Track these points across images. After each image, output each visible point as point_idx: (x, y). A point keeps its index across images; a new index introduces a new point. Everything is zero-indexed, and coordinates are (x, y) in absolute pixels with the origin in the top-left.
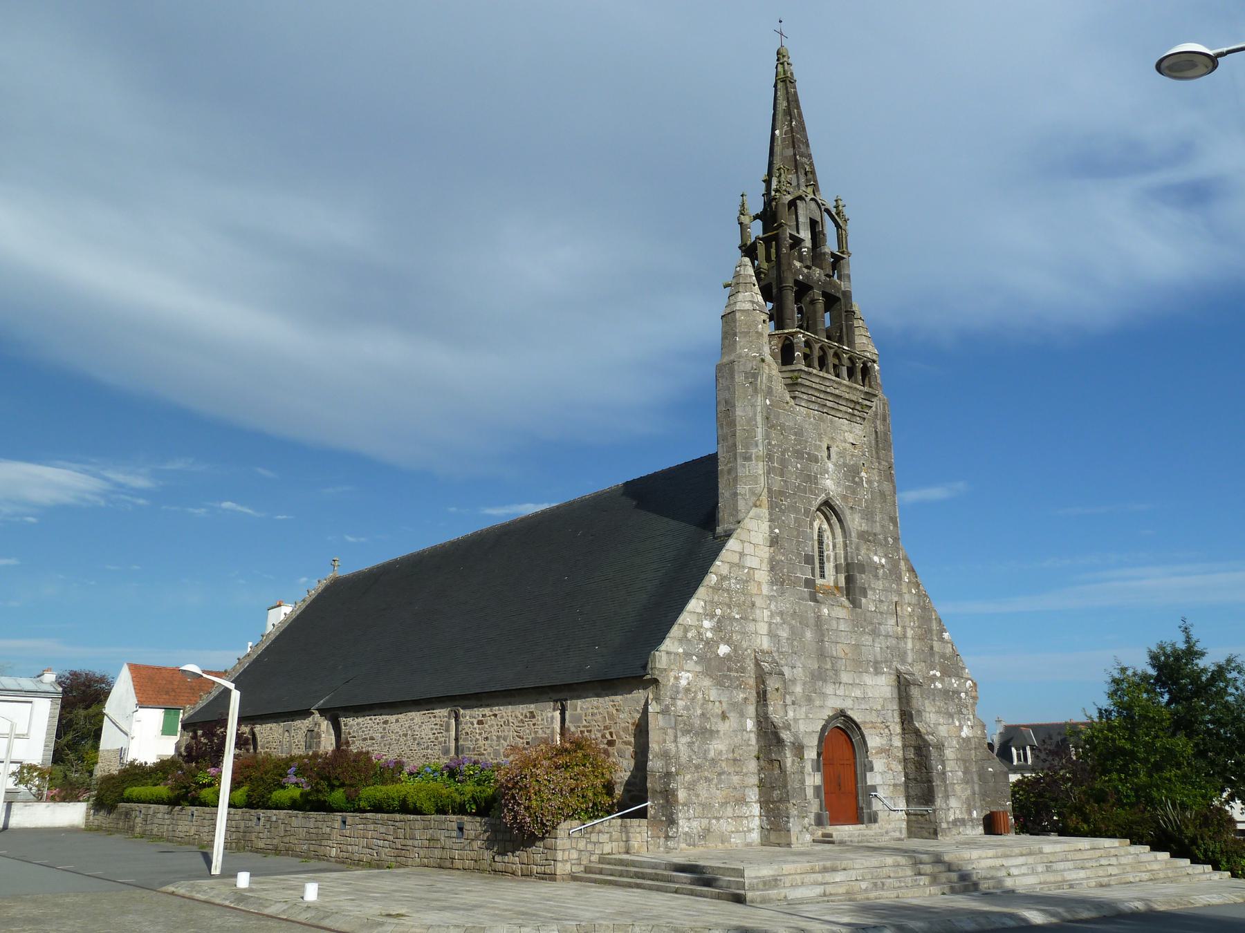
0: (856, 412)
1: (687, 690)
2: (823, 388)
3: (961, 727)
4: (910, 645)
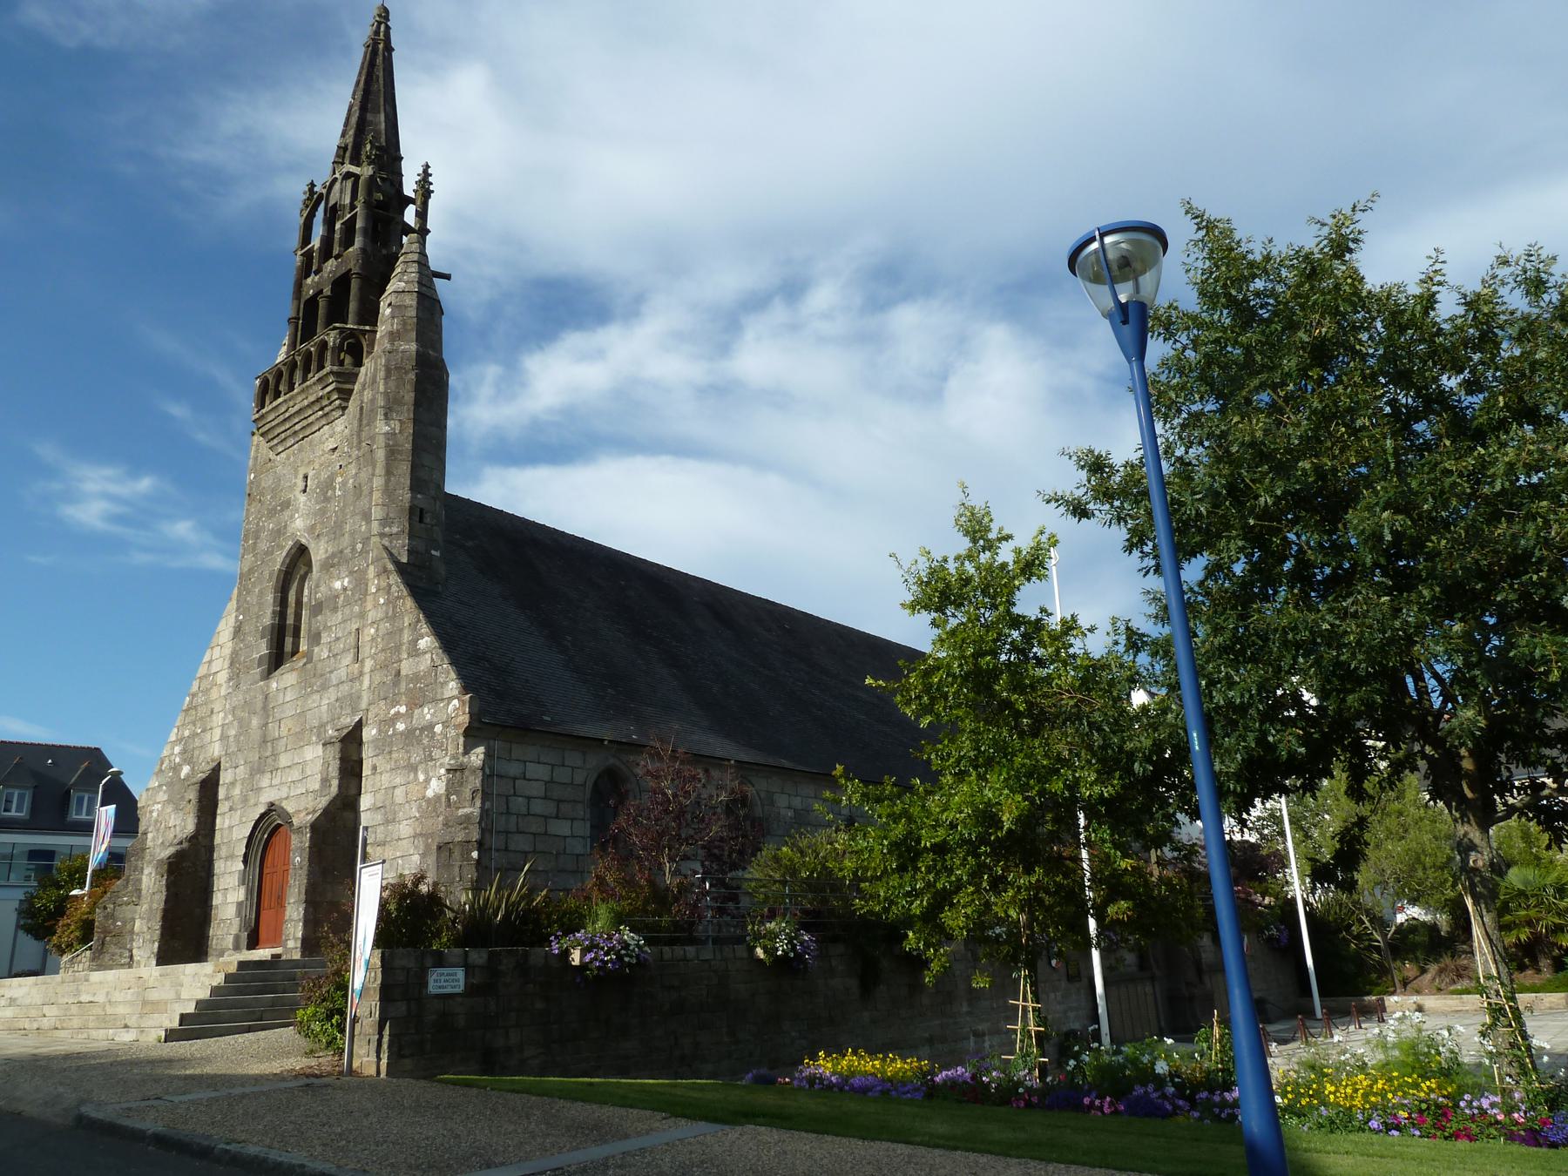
0: (327, 409)
1: (156, 821)
2: (282, 418)
3: (427, 781)
4: (366, 683)
